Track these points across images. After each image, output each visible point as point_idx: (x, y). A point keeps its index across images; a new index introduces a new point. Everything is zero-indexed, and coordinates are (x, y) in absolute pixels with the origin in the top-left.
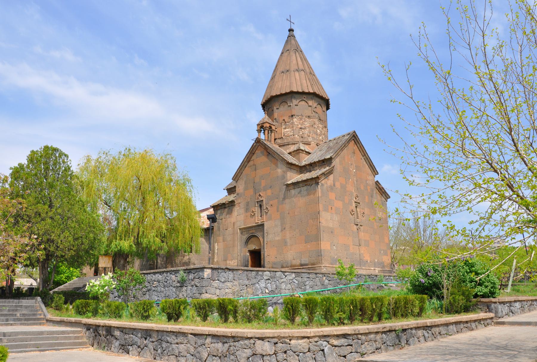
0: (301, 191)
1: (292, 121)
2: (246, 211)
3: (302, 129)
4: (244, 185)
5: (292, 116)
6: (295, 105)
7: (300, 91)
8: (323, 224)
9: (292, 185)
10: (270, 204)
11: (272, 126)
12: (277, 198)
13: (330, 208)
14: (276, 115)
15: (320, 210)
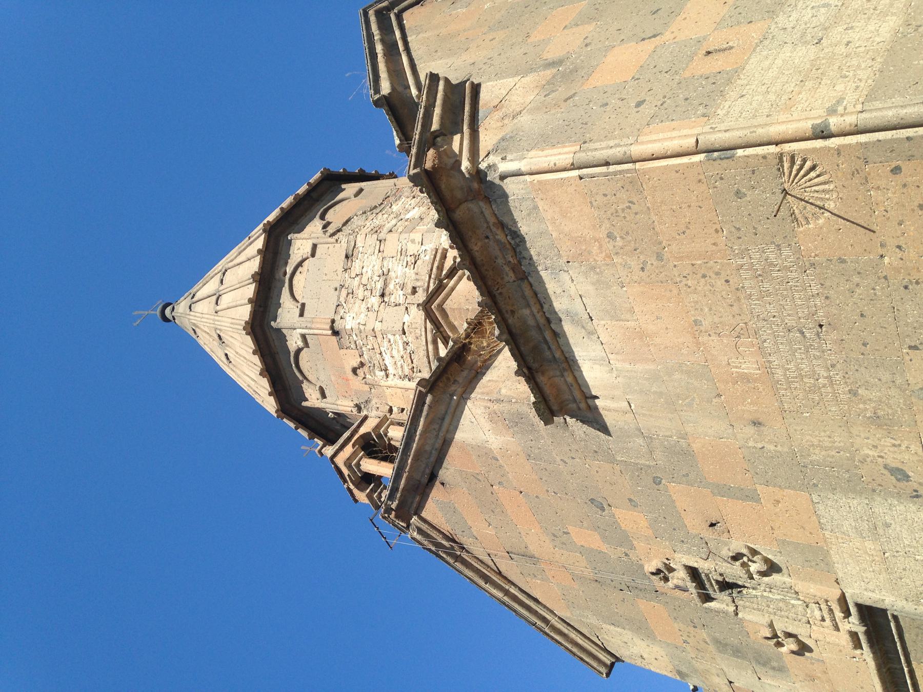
0: (577, 322)
1: (354, 336)
2: (773, 668)
3: (387, 292)
4: (628, 635)
5: (336, 333)
6: (301, 315)
7: (250, 290)
8: (850, 97)
9: (542, 379)
10: (708, 534)
11: (362, 430)
12: (657, 481)
13: (718, 63)
14: (345, 406)
15: (690, 143)
